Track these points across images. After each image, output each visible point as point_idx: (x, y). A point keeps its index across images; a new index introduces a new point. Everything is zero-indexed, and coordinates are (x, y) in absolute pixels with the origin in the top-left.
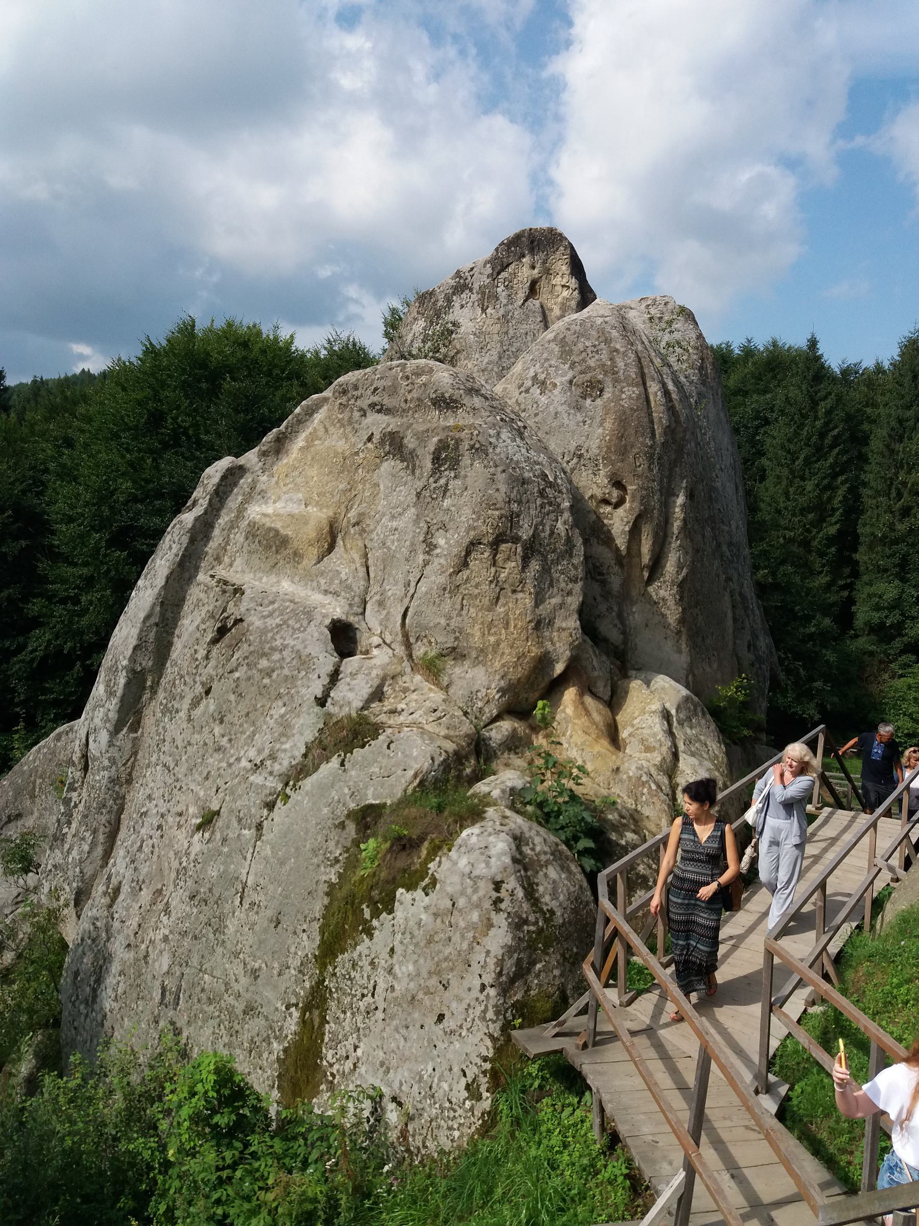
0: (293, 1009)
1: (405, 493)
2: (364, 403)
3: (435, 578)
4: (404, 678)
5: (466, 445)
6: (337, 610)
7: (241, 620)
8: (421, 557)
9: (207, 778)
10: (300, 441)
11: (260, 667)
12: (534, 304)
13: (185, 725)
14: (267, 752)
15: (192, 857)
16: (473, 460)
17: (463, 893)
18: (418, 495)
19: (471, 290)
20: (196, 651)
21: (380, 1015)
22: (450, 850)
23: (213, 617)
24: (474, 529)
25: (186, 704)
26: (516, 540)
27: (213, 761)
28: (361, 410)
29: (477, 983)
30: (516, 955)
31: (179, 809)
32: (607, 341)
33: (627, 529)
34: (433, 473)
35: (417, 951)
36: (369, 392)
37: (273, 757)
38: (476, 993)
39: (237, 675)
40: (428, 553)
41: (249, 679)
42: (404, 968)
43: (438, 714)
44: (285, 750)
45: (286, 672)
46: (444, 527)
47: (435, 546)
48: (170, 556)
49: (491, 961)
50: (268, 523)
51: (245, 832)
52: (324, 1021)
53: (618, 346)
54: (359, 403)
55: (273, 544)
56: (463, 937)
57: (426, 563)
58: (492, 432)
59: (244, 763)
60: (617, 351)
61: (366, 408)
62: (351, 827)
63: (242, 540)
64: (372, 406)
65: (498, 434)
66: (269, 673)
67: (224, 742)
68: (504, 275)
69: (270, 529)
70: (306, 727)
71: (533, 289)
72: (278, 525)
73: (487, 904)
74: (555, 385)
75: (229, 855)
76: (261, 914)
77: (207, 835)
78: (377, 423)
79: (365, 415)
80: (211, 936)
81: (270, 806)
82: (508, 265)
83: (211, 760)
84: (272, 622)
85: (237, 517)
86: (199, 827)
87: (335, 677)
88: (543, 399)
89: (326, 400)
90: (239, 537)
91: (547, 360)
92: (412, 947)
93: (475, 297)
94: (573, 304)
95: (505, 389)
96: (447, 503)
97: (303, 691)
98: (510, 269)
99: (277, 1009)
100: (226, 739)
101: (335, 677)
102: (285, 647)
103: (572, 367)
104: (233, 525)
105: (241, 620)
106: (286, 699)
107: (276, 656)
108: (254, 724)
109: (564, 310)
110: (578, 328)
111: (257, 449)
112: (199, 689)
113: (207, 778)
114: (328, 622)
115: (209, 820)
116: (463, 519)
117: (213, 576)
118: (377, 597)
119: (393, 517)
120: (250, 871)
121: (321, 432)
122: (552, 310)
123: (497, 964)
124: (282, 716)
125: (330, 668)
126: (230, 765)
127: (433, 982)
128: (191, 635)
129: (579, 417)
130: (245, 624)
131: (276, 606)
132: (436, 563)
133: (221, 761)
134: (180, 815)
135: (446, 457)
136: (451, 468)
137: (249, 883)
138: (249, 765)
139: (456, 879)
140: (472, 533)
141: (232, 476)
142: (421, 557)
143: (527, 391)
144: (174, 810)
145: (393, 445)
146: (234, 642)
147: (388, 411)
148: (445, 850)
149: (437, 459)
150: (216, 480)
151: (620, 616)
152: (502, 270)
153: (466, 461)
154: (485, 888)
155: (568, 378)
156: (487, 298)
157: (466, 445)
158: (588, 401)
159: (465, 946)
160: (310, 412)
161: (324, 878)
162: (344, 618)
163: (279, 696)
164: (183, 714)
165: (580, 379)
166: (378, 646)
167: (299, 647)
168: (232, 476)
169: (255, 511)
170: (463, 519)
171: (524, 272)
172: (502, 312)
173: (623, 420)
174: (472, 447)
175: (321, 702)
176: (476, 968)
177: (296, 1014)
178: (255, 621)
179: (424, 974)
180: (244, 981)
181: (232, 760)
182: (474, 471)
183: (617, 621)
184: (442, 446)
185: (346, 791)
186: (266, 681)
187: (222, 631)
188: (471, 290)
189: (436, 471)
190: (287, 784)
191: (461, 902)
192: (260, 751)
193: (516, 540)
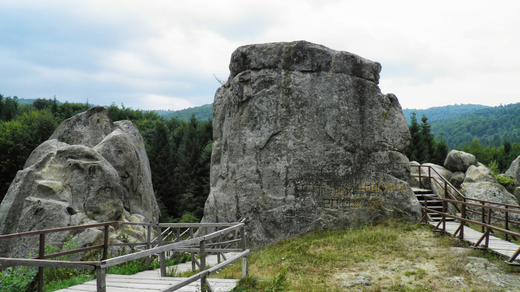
3: (92, 196)
8: (87, 192)
18: (85, 178)
26: (110, 187)
46: (92, 185)
55: (47, 191)
57: (89, 193)
66: (52, 220)
96: (93, 180)
119: (78, 183)
132: (91, 194)
142: (87, 192)
151: (129, 202)
169: (40, 182)
171: (95, 117)
184: (90, 168)
189: (90, 173)
193: (110, 187)
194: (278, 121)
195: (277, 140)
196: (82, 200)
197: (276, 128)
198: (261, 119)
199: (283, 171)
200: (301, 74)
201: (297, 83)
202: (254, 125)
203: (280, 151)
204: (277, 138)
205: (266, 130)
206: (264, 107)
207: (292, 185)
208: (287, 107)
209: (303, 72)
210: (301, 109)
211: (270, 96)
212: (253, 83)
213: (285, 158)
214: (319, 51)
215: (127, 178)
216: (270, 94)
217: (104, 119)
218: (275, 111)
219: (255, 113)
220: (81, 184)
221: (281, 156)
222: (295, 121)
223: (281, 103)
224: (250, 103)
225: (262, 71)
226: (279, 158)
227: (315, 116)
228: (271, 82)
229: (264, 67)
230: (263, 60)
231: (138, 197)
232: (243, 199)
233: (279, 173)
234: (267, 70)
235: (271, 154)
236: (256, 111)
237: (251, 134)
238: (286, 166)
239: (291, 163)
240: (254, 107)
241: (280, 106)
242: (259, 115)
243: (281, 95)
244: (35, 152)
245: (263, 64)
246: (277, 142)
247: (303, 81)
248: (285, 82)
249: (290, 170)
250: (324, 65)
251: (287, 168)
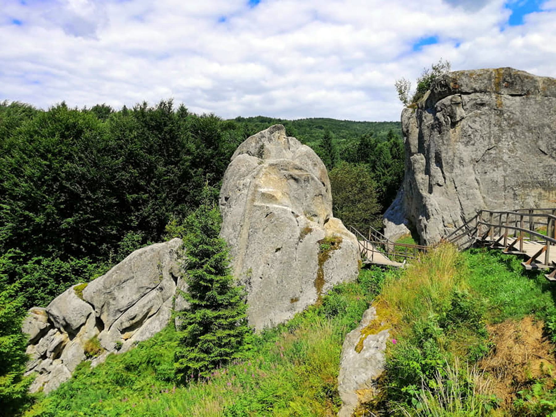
25: (262, 230)
66: (282, 222)
81: (298, 244)
93: (267, 139)
135: (307, 180)
147: (285, 170)
153: (310, 181)
173: (322, 171)
194: (492, 138)
195: (491, 153)
197: (490, 143)
198: (475, 136)
199: (500, 179)
200: (510, 97)
201: (508, 105)
202: (469, 142)
203: (496, 164)
204: (492, 152)
205: (482, 146)
206: (477, 126)
207: (511, 190)
208: (500, 126)
209: (512, 95)
210: (513, 128)
211: (483, 117)
212: (465, 105)
213: (501, 168)
214: (527, 77)
216: (483, 115)
218: (488, 129)
219: (468, 131)
220: (298, 192)
221: (497, 167)
222: (507, 138)
223: (494, 123)
224: (463, 122)
225: (473, 94)
226: (496, 169)
227: (526, 134)
228: (483, 105)
229: (475, 91)
230: (474, 86)
232: (465, 203)
233: (497, 181)
234: (478, 94)
235: (488, 166)
236: (470, 129)
237: (466, 149)
238: (503, 176)
239: (507, 173)
240: (468, 126)
241: (492, 125)
242: (472, 133)
243: (493, 116)
244: (231, 165)
245: (475, 89)
246: (493, 156)
247: (513, 103)
248: (496, 105)
249: (507, 178)
250: (533, 89)
251: (504, 177)
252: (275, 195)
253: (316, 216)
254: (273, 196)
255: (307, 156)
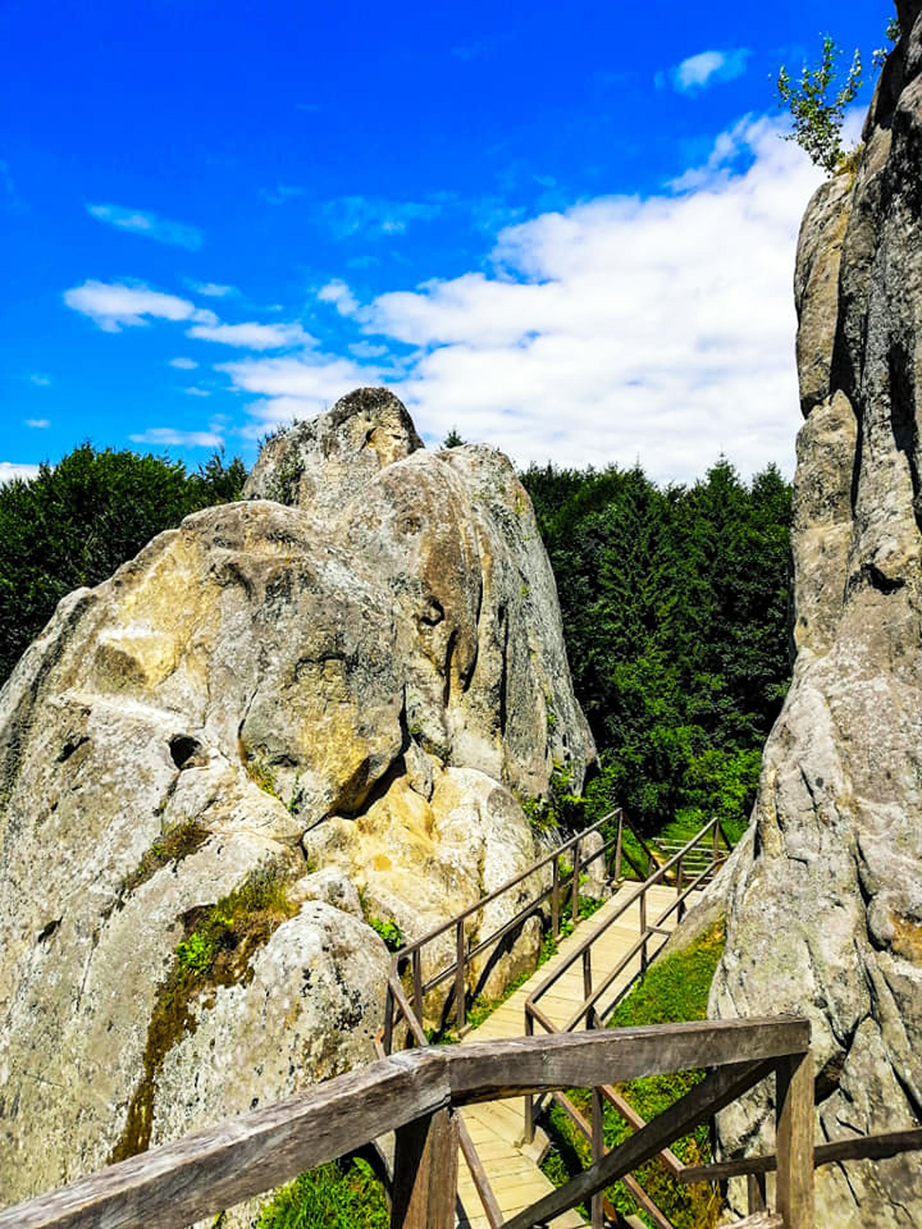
0: (123, 1109)
1: (242, 617)
2: (209, 538)
4: (239, 787)
5: (296, 574)
6: (178, 726)
7: (87, 739)
8: (256, 674)
9: (50, 891)
10: (151, 573)
11: (102, 782)
12: (371, 450)
13: (31, 840)
14: (106, 863)
15: (33, 968)
16: (303, 588)
17: (276, 983)
18: (254, 618)
19: (315, 439)
20: (44, 770)
21: (201, 1105)
22: (266, 944)
23: (61, 737)
24: (302, 647)
25: (33, 820)
26: (341, 656)
27: (58, 873)
28: (205, 542)
29: (287, 1065)
30: (323, 1037)
31: (23, 922)
32: (424, 485)
33: (445, 643)
34: (267, 600)
35: (236, 1041)
36: (213, 529)
37: (111, 867)
38: (286, 1076)
39: (81, 790)
40: (262, 670)
41: (92, 794)
42: (223, 1058)
43: (267, 818)
44: (121, 860)
45: (127, 786)
47: (269, 665)
48: (23, 680)
49: (300, 1043)
50: (118, 647)
51: (83, 940)
52: (151, 1117)
53: (433, 489)
54: (204, 537)
56: (275, 1023)
57: (261, 680)
58: (320, 563)
59: (86, 874)
60: (432, 493)
61: (211, 542)
62: (180, 927)
63: (92, 663)
64: (216, 540)
65: (326, 564)
66: (110, 787)
67: (68, 855)
68: (343, 426)
69: (118, 652)
70: (145, 839)
71: (369, 437)
72: (126, 650)
73: (297, 992)
74: (380, 522)
75: (68, 963)
76: (96, 1018)
77: (48, 945)
78: (221, 554)
79: (209, 548)
80: (49, 1042)
81: (106, 914)
82: (347, 418)
83: (54, 874)
84: (115, 739)
85: (89, 642)
86: (41, 938)
87: (172, 789)
88: (371, 534)
89: (174, 535)
90: (89, 660)
91: (373, 500)
92: (230, 1038)
93: (318, 444)
94: (404, 451)
95: (338, 525)
96: (280, 625)
97: (142, 803)
98: (348, 422)
99: (108, 1110)
100: (70, 852)
101: (172, 789)
102: (127, 762)
103: (394, 507)
104: (83, 650)
105: (87, 739)
106: (125, 811)
107: (119, 771)
108: (95, 836)
109: (397, 456)
110: (399, 474)
111: (110, 580)
112: (46, 805)
113: (50, 891)
114: (168, 737)
115: (50, 929)
116: (294, 639)
117: (62, 699)
118: (216, 712)
119: (232, 639)
120: (86, 978)
121: (170, 565)
122: (385, 456)
123: (305, 1047)
124: (122, 828)
125: (168, 781)
126: (72, 877)
127: (250, 1068)
128: (39, 755)
129: (402, 548)
130: (90, 742)
131: (121, 723)
133: (64, 873)
134: (25, 927)
136: (282, 595)
137: (87, 991)
138: (89, 876)
139: (270, 971)
140: (301, 652)
141: (84, 605)
142: (256, 674)
143: (357, 526)
144: (19, 923)
145: (234, 575)
146: (80, 759)
147: (231, 545)
148: (262, 945)
149: (271, 589)
150: (70, 609)
152: (343, 422)
154: (296, 978)
155: (391, 515)
156: (329, 445)
157: (296, 574)
158: (409, 534)
159: (277, 1032)
160: (162, 546)
161: (153, 979)
162: (184, 732)
163: (121, 808)
164: (30, 831)
165: (401, 516)
166: (216, 757)
167: (141, 762)
168: (84, 605)
169: (105, 637)
170: (294, 639)
171: (360, 424)
172: (342, 457)
174: (302, 576)
175: (158, 812)
176: (286, 1051)
177: (125, 1112)
178: (100, 739)
179: (241, 1062)
180: (78, 1084)
181: (74, 872)
182: (303, 596)
183: (439, 725)
185: (177, 895)
186: (109, 795)
187: (68, 751)
188: (315, 439)
190: (122, 893)
191: (275, 992)
192: (100, 862)
193: (341, 656)
196: (235, 705)
215: (433, 624)
217: (389, 431)
231: (478, 698)
252: (139, 657)
253: (295, 764)
254: (132, 663)
255: (386, 486)
